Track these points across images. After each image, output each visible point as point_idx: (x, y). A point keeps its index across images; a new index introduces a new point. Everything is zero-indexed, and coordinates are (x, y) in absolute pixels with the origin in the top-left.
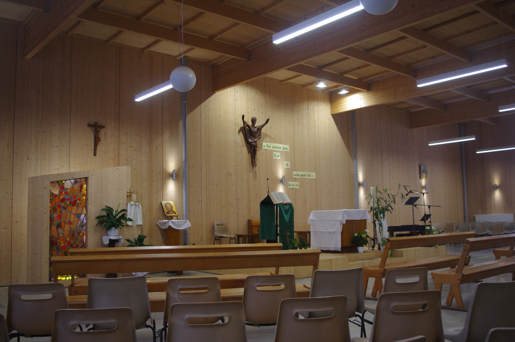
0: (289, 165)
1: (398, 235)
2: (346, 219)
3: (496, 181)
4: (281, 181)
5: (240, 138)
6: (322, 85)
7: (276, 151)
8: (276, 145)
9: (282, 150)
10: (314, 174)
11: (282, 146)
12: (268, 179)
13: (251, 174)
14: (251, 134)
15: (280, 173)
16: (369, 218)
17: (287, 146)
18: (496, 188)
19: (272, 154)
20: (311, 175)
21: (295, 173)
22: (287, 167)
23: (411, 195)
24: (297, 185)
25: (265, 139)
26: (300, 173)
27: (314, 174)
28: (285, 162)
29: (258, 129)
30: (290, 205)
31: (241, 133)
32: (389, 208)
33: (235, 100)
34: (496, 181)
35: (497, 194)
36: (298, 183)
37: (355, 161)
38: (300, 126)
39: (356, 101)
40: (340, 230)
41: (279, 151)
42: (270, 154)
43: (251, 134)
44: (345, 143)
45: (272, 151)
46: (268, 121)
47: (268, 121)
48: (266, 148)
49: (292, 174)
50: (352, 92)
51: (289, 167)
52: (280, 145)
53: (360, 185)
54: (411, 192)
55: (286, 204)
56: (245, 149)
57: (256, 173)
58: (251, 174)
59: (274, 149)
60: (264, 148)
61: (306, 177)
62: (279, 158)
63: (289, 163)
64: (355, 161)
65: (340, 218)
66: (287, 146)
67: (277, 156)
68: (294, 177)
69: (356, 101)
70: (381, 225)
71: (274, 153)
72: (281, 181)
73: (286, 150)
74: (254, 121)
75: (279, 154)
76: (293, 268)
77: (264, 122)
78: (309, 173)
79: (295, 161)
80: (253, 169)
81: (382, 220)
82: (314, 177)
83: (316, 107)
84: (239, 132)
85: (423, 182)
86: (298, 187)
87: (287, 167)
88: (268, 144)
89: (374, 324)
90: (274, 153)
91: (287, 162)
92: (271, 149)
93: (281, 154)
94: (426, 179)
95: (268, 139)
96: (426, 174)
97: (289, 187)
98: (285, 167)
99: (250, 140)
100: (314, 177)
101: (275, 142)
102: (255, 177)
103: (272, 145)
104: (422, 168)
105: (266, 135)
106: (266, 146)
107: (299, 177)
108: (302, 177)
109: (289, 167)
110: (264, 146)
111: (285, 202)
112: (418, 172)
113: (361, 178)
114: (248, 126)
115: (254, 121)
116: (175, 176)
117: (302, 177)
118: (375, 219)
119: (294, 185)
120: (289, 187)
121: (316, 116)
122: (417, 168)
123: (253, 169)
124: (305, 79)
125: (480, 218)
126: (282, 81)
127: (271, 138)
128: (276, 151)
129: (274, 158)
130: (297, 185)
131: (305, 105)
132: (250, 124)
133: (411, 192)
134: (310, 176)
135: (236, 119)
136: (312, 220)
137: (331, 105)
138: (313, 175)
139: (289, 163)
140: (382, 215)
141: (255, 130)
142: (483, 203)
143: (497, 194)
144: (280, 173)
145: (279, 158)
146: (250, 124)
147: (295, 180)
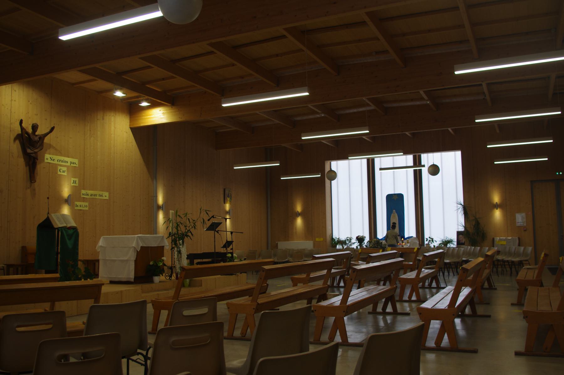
0: (77, 182)
1: (198, 263)
2: (141, 245)
4: (67, 201)
5: (16, 148)
6: (119, 94)
7: (61, 166)
8: (62, 158)
9: (69, 164)
10: (106, 195)
12: (48, 198)
13: (29, 191)
15: (66, 192)
16: (167, 244)
17: (76, 161)
19: (57, 168)
20: (104, 196)
21: (83, 192)
22: (74, 185)
23: (213, 220)
24: (86, 206)
25: (48, 151)
26: (90, 192)
27: (107, 194)
28: (73, 179)
29: (40, 138)
30: (74, 229)
31: (17, 142)
32: (190, 234)
33: (12, 100)
36: (87, 204)
37: (155, 182)
38: (92, 138)
39: (158, 116)
40: (133, 258)
42: (54, 168)
44: (144, 160)
45: (56, 165)
46: (52, 129)
47: (52, 129)
48: (49, 161)
49: (80, 193)
50: (154, 105)
51: (77, 185)
52: (66, 159)
53: (159, 208)
54: (213, 217)
55: (70, 228)
56: (21, 161)
57: (34, 190)
58: (29, 191)
59: (59, 163)
60: (46, 161)
61: (98, 197)
62: (65, 174)
63: (77, 180)
64: (155, 182)
65: (134, 245)
67: (63, 171)
68: (82, 196)
69: (158, 116)
70: (179, 252)
71: (59, 168)
72: (67, 201)
73: (74, 165)
74: (35, 127)
75: (65, 169)
76: (75, 302)
77: (48, 130)
78: (101, 193)
80: (30, 186)
81: (181, 247)
83: (113, 119)
84: (15, 139)
85: (227, 207)
86: (87, 209)
87: (74, 185)
88: (51, 156)
90: (59, 168)
92: (56, 162)
93: (68, 169)
94: (230, 204)
95: (52, 150)
96: (231, 199)
97: (76, 208)
98: (72, 185)
99: (29, 151)
100: (107, 198)
101: (61, 155)
103: (57, 158)
104: (227, 192)
105: (50, 146)
106: (49, 159)
109: (77, 185)
110: (47, 159)
111: (69, 226)
112: (222, 196)
113: (160, 200)
114: (27, 133)
115: (35, 127)
118: (173, 246)
119: (82, 205)
120: (76, 208)
121: (113, 128)
122: (222, 192)
123: (30, 186)
124: (100, 84)
126: (73, 84)
127: (56, 149)
128: (61, 166)
129: (59, 173)
130: (86, 206)
132: (30, 131)
133: (213, 217)
134: (101, 196)
135: (11, 124)
136: (101, 246)
137: (130, 118)
138: (106, 195)
139: (77, 180)
140: (181, 241)
141: (37, 139)
142: (286, 230)
144: (66, 192)
145: (65, 174)
146: (30, 131)
147: (84, 200)
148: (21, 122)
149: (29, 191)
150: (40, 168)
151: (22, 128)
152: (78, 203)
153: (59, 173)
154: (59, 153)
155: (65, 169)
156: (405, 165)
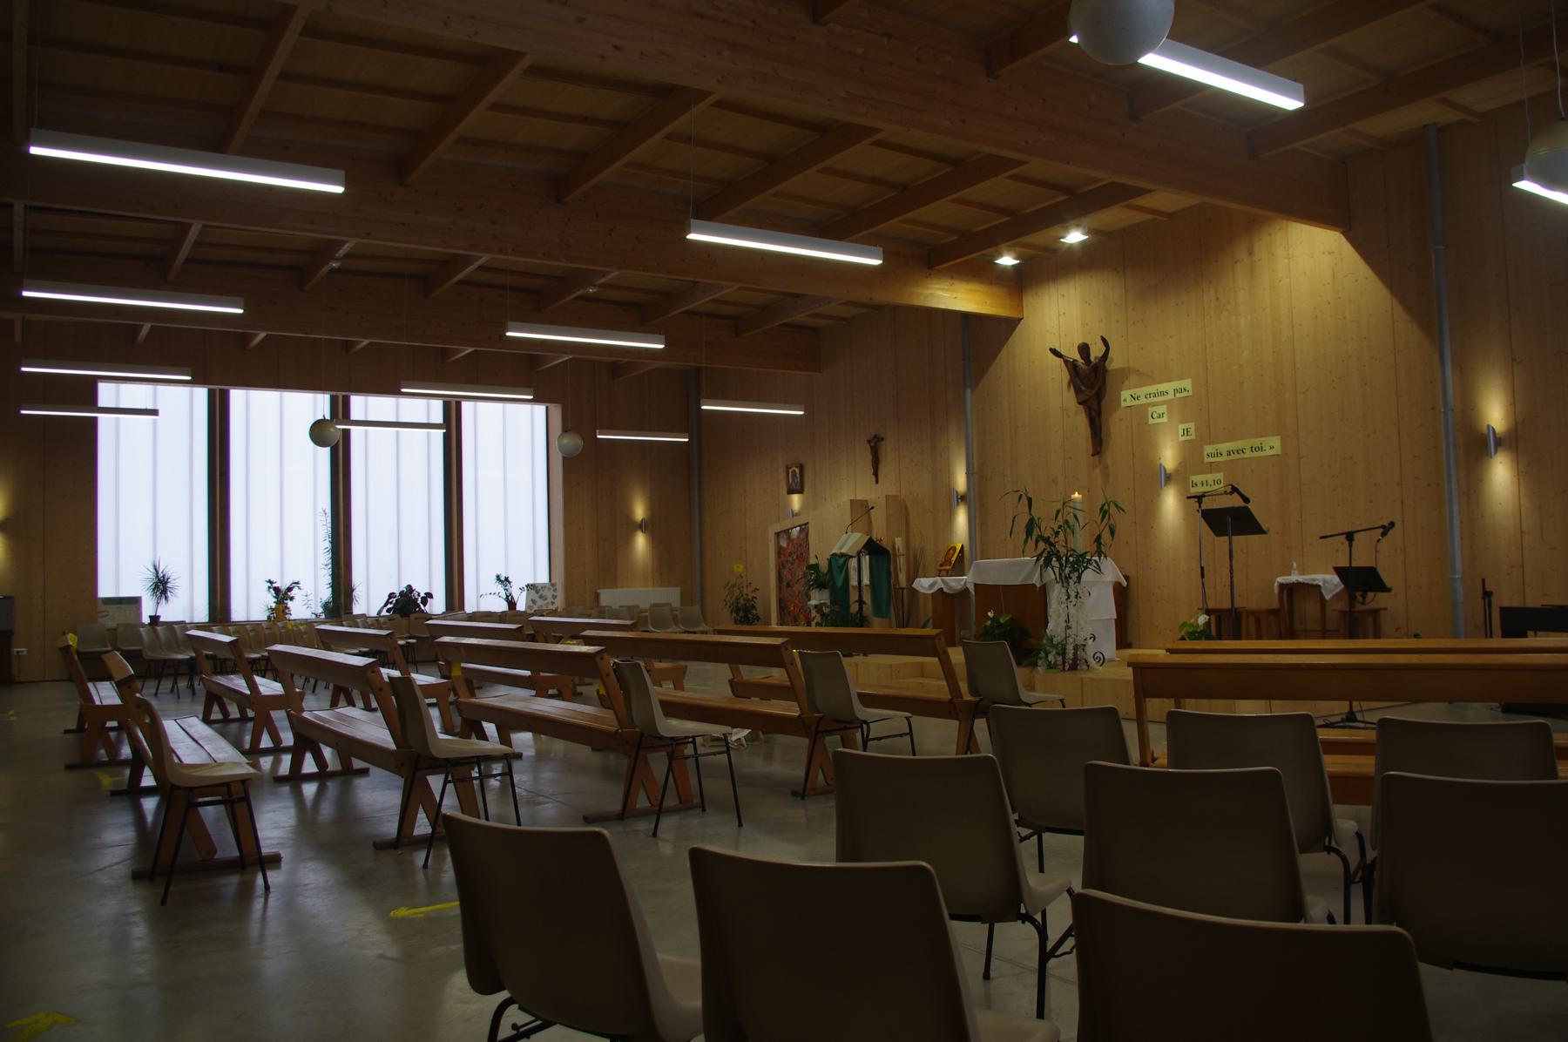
0: (1192, 431)
3: (639, 511)
5: (1070, 397)
7: (1154, 404)
8: (1153, 389)
9: (1170, 396)
10: (1275, 441)
11: (1169, 387)
14: (1091, 379)
15: (1169, 457)
17: (1187, 384)
18: (641, 526)
20: (1266, 447)
21: (1209, 449)
24: (1219, 482)
26: (1224, 447)
27: (1275, 441)
28: (1182, 426)
34: (639, 511)
35: (641, 542)
36: (1220, 476)
42: (1140, 412)
43: (1091, 379)
44: (1408, 309)
52: (1162, 387)
56: (1082, 420)
57: (1106, 467)
58: (1097, 471)
60: (1123, 404)
61: (1248, 454)
63: (1191, 426)
66: (1187, 384)
67: (1160, 415)
71: (1151, 410)
74: (1084, 349)
75: (1163, 409)
78: (1256, 442)
79: (1207, 415)
88: (1132, 392)
90: (1151, 410)
92: (1143, 401)
95: (1133, 379)
100: (1277, 450)
101: (1154, 381)
102: (1106, 476)
105: (1125, 373)
107: (1225, 458)
108: (1233, 457)
116: (1511, 442)
117: (1233, 457)
119: (1205, 482)
125: (609, 597)
127: (1138, 373)
128: (1154, 404)
129: (1151, 421)
134: (1261, 449)
138: (1273, 445)
139: (1191, 426)
143: (641, 542)
144: (1169, 457)
145: (1165, 419)
147: (1212, 468)
148: (1054, 352)
149: (1097, 471)
150: (1116, 427)
151: (1066, 362)
152: (1197, 478)
153: (1151, 421)
154: (1147, 378)
155: (1163, 409)
156: (393, 419)
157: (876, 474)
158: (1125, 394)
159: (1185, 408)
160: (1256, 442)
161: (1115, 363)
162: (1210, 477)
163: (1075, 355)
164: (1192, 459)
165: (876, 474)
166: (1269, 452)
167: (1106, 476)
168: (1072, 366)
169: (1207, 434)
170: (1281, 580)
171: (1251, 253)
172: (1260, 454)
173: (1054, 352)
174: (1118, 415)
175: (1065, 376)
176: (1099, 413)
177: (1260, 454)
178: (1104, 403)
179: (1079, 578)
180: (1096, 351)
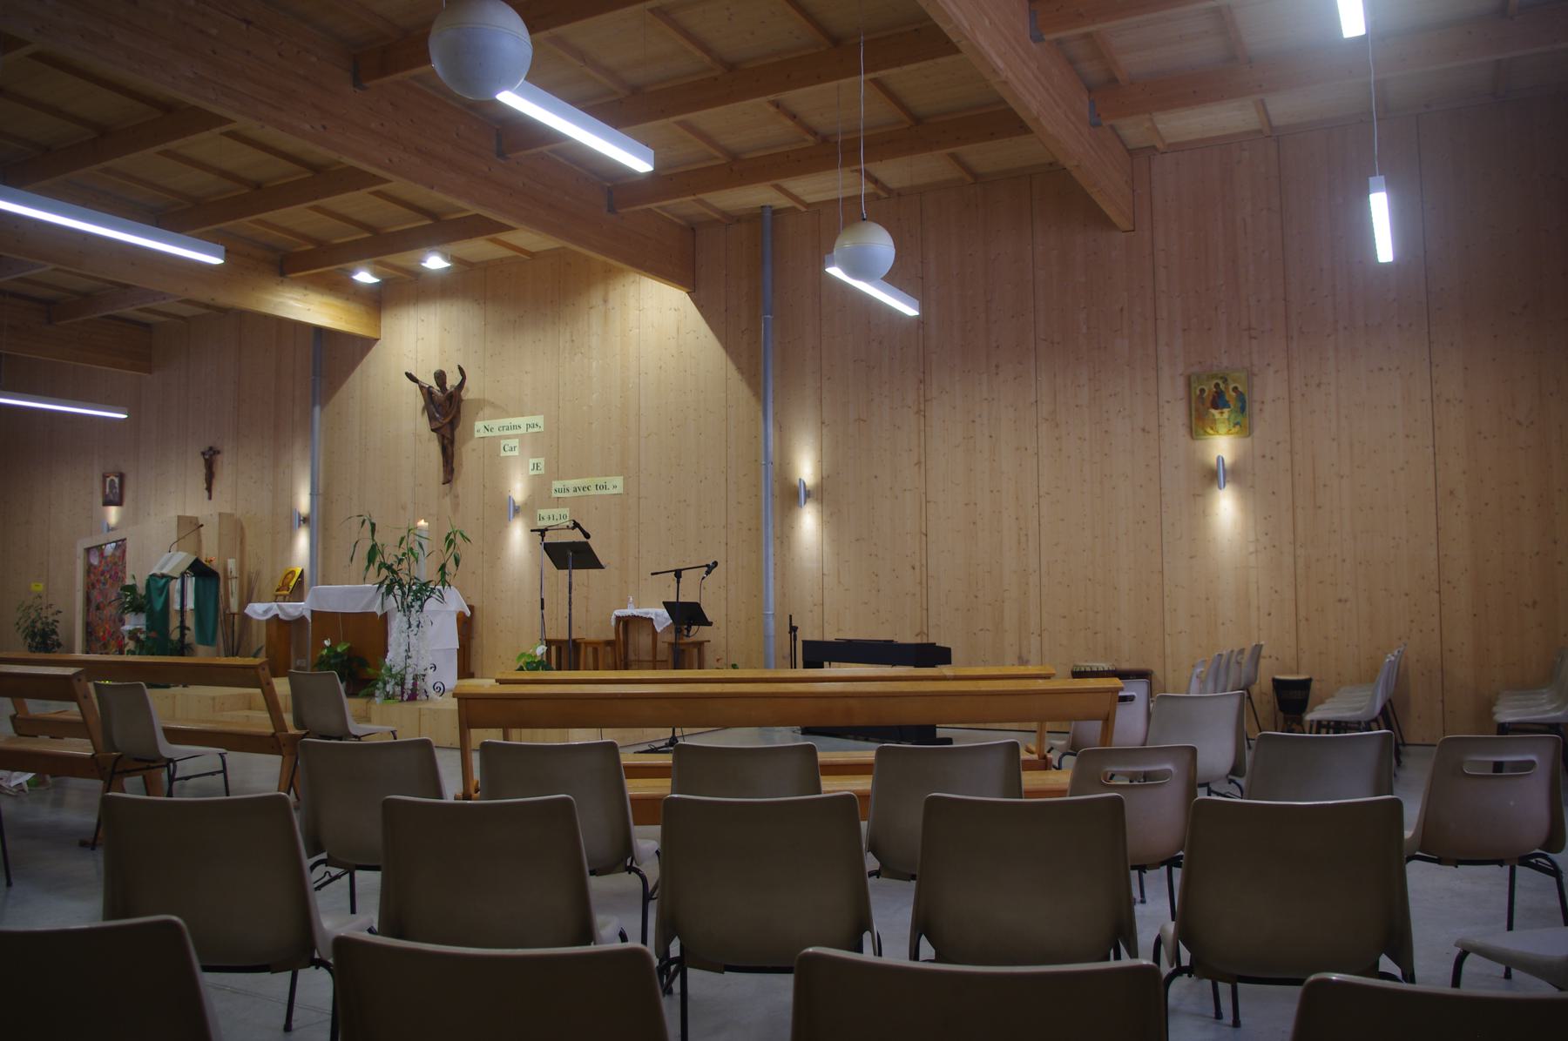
0: (542, 466)
5: (423, 423)
8: (506, 422)
9: (523, 430)
11: (521, 421)
15: (518, 490)
17: (539, 420)
21: (557, 484)
26: (571, 483)
28: (532, 461)
36: (565, 511)
41: (515, 436)
42: (493, 444)
43: (445, 407)
44: (739, 369)
49: (549, 489)
56: (434, 448)
57: (457, 497)
58: (448, 499)
60: (477, 435)
61: (593, 492)
66: (539, 420)
67: (511, 449)
68: (555, 495)
71: (503, 442)
74: (440, 377)
75: (515, 442)
78: (600, 481)
79: (559, 453)
82: (620, 490)
88: (486, 423)
89: (1454, 991)
90: (503, 442)
91: (536, 461)
92: (496, 433)
93: (522, 444)
95: (487, 411)
100: (620, 490)
101: (508, 415)
102: (455, 507)
103: (495, 423)
105: (480, 404)
107: (571, 494)
108: (579, 493)
115: (440, 377)
116: (819, 494)
117: (579, 493)
127: (493, 405)
129: (503, 454)
131: (596, 297)
138: (616, 484)
139: (541, 461)
144: (518, 490)
145: (516, 453)
147: (558, 503)
148: (409, 376)
149: (448, 499)
150: (468, 456)
151: (421, 387)
152: (543, 512)
153: (503, 454)
154: (502, 411)
157: (209, 489)
158: (479, 425)
159: (535, 443)
160: (600, 481)
161: (469, 394)
162: (556, 512)
163: (430, 381)
164: (541, 493)
165: (209, 489)
166: (615, 491)
167: (455, 507)
168: (427, 393)
169: (556, 470)
170: (618, 612)
171: (605, 301)
172: (604, 492)
173: (409, 376)
174: (470, 445)
175: (420, 401)
176: (452, 442)
177: (604, 492)
178: (457, 433)
179: (421, 607)
180: (452, 380)
